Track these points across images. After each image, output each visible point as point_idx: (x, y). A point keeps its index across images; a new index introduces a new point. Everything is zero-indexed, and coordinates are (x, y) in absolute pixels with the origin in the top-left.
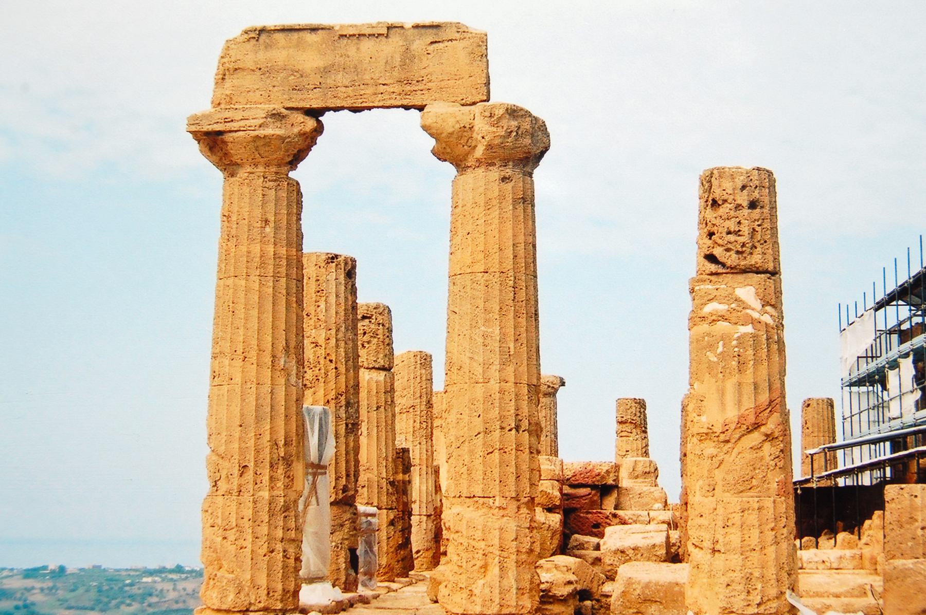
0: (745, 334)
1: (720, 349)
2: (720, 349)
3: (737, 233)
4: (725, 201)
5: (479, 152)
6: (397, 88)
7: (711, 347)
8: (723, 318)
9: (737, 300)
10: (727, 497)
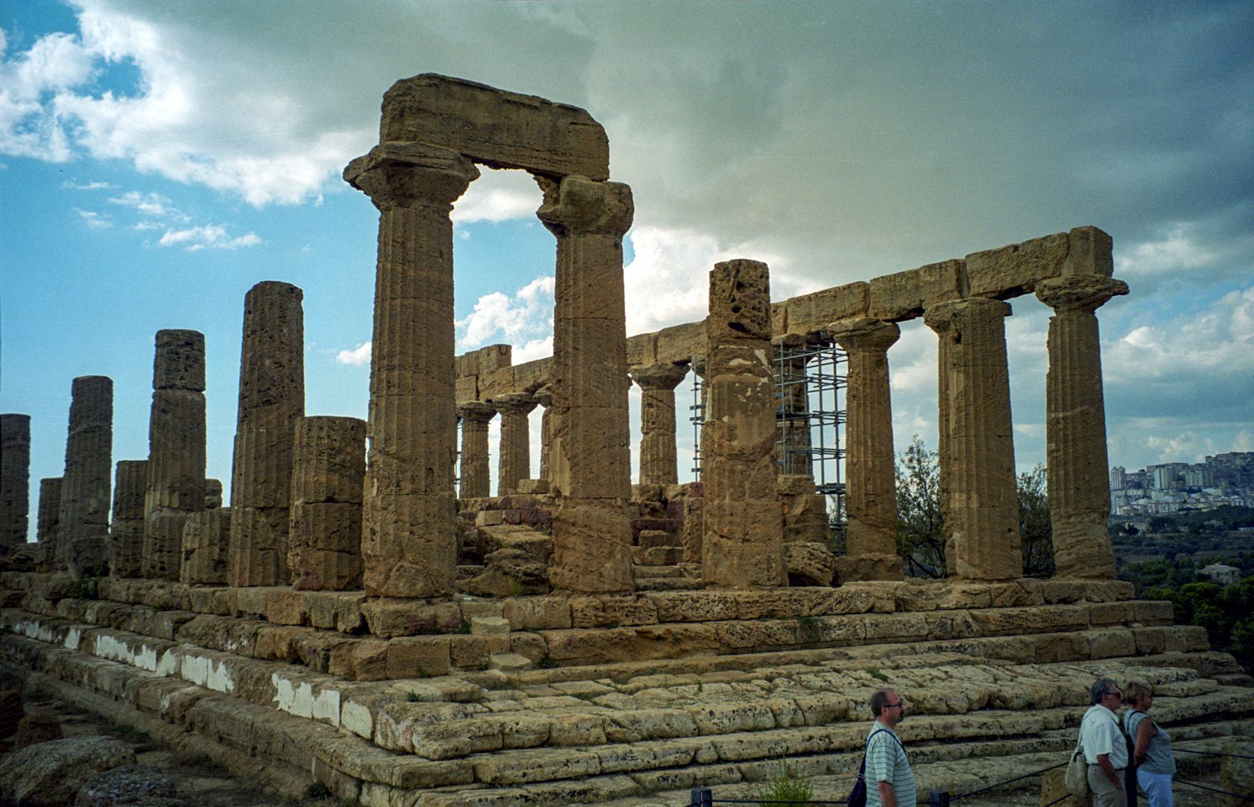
0: (764, 384)
1: (749, 393)
2: (749, 393)
3: (759, 310)
4: (751, 285)
5: (603, 220)
6: (547, 156)
7: (743, 391)
8: (749, 370)
9: (757, 359)
10: (752, 501)
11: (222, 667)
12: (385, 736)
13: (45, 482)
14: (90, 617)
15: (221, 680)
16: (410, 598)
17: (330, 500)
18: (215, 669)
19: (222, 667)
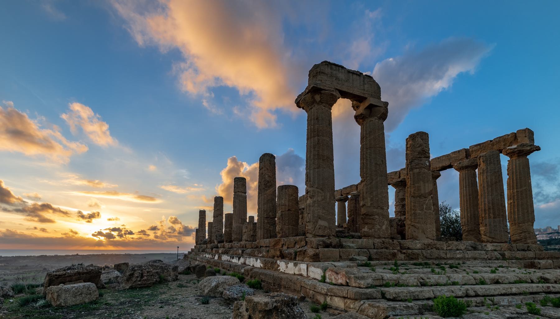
11: (259, 261)
12: (330, 279)
13: (209, 223)
14: (220, 252)
15: (258, 264)
16: (322, 236)
17: (289, 210)
18: (256, 261)
19: (259, 261)
